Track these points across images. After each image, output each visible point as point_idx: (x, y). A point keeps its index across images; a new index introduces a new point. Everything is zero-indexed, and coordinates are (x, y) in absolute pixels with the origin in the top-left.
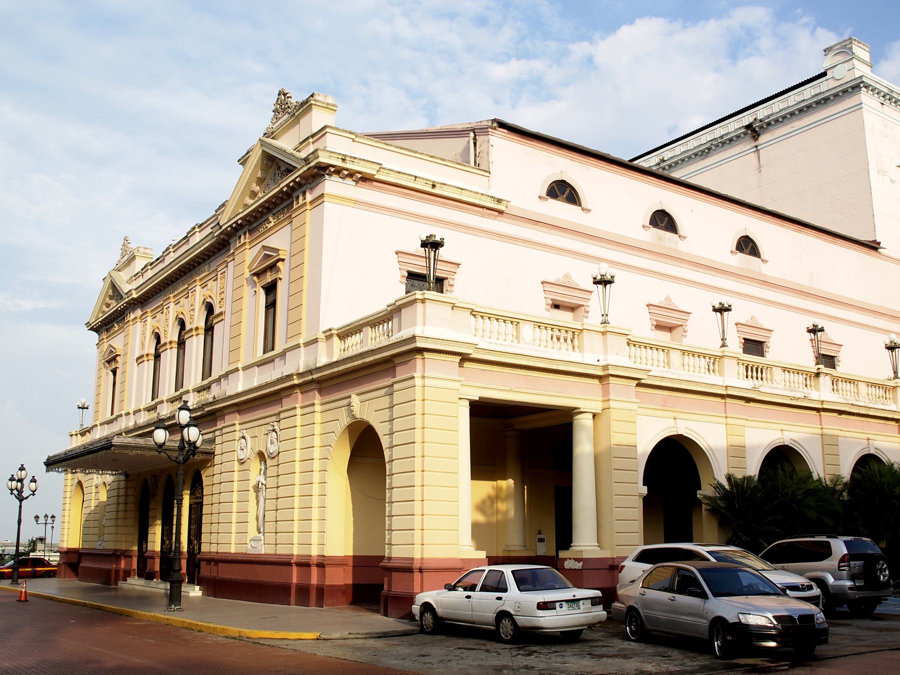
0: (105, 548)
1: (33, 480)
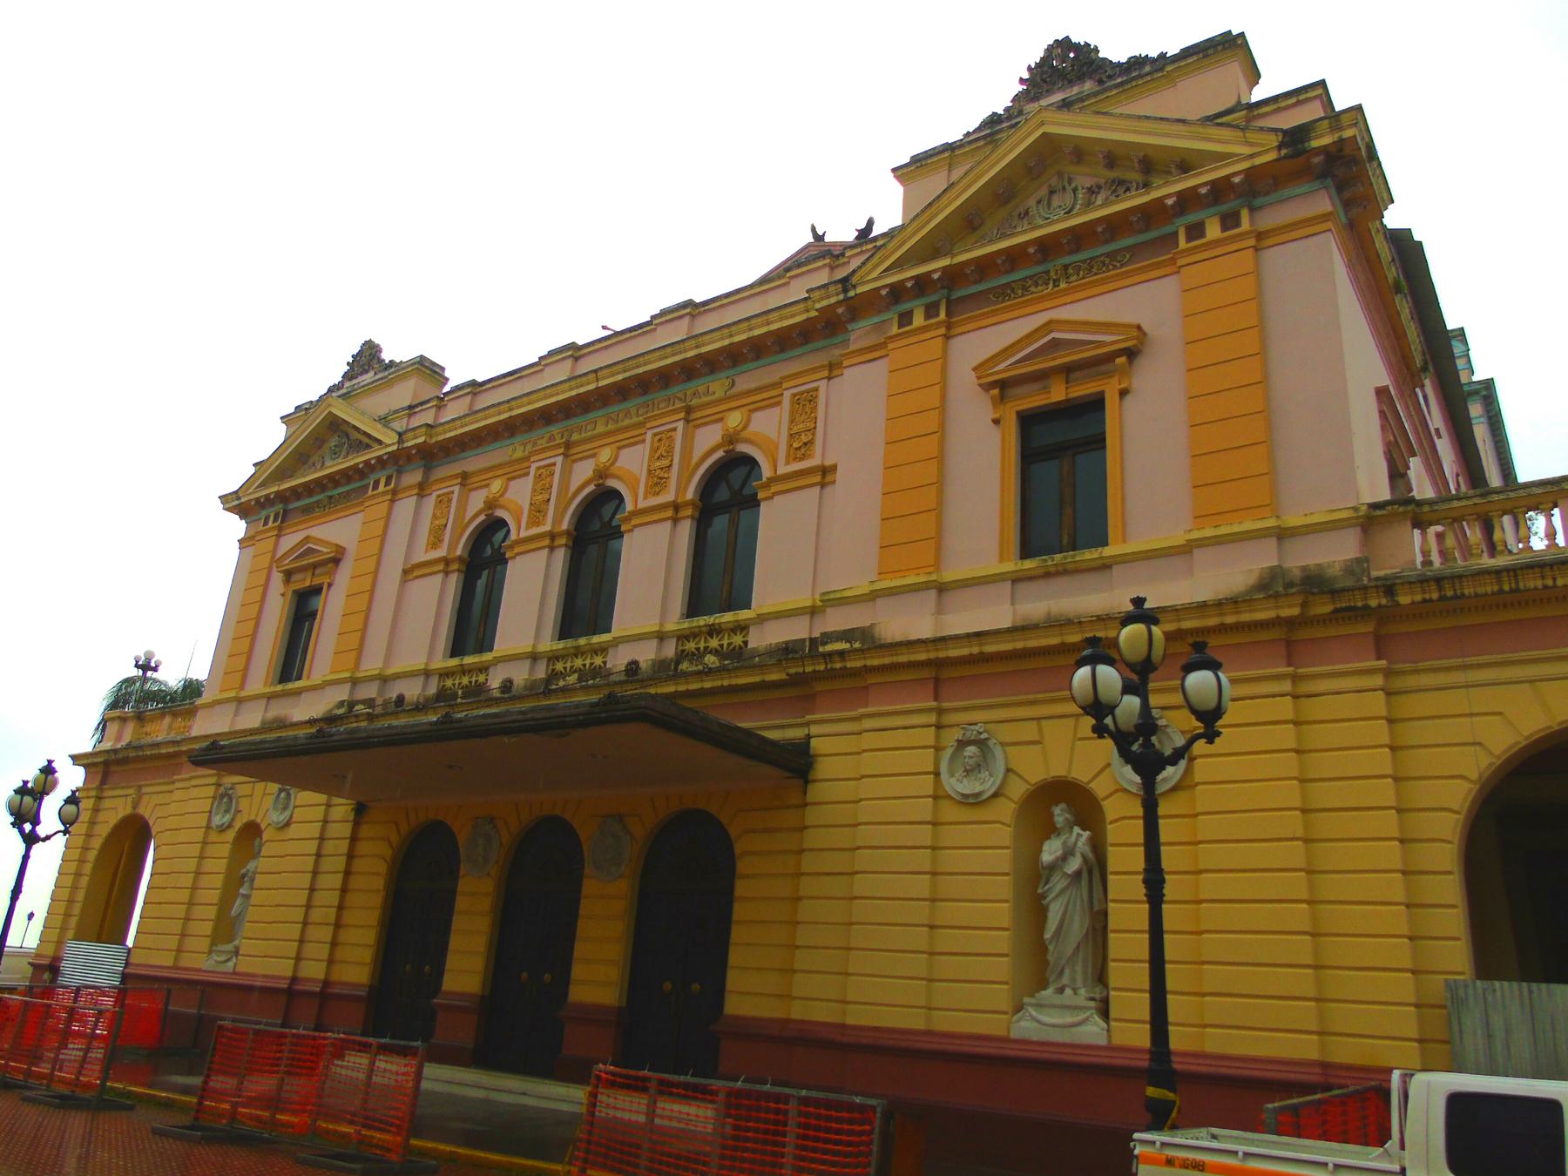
0: (237, 970)
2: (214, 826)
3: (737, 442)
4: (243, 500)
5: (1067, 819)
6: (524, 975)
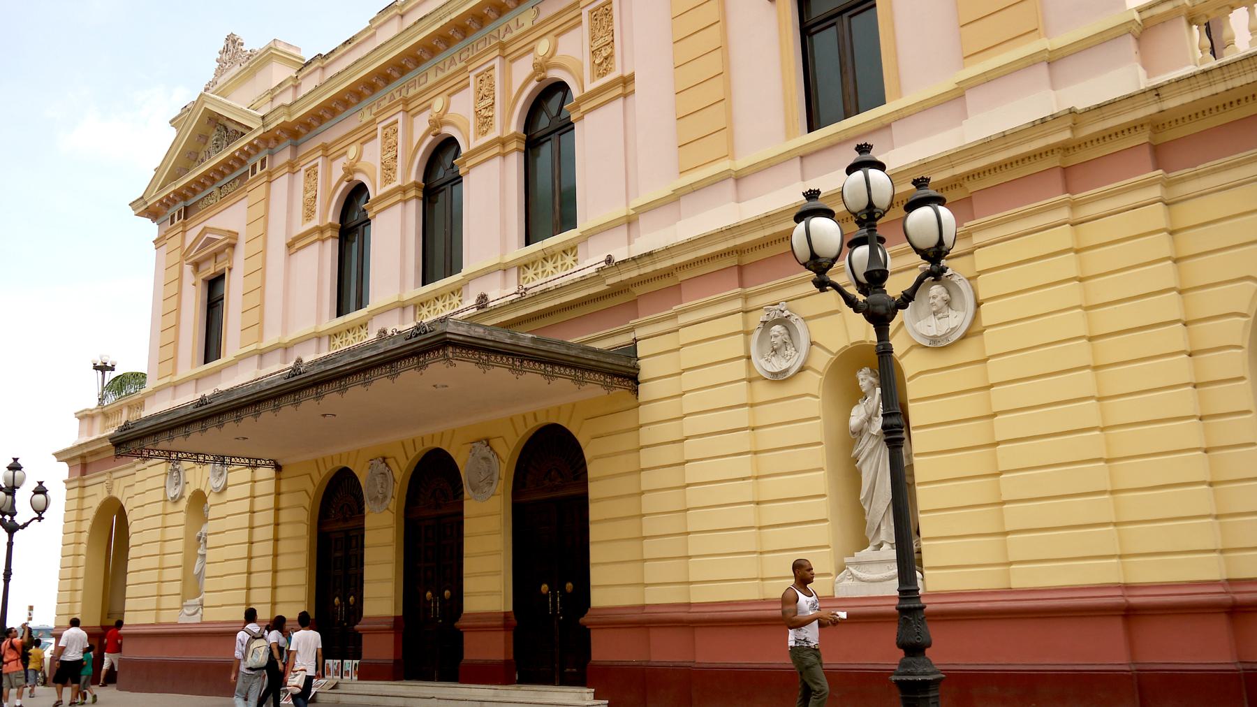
0: (204, 620)
1: (41, 490)
2: (170, 499)
3: (548, 68)
4: (148, 204)
5: (871, 382)
6: (429, 594)
